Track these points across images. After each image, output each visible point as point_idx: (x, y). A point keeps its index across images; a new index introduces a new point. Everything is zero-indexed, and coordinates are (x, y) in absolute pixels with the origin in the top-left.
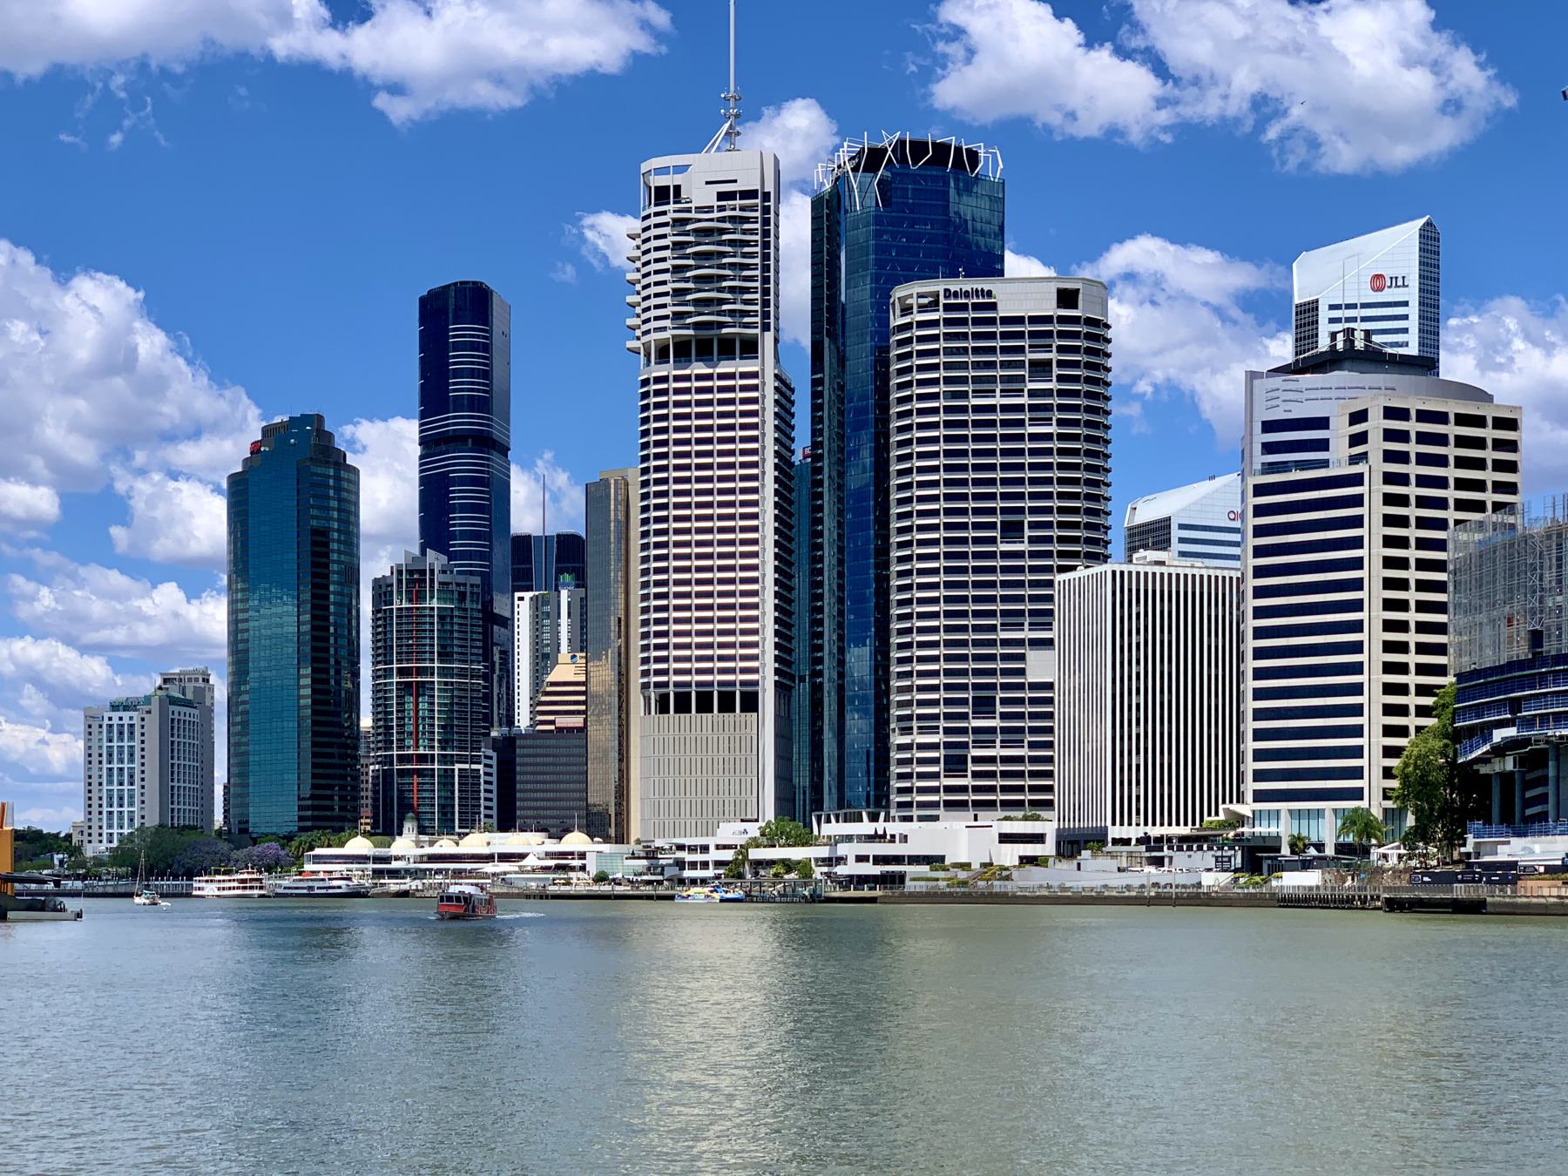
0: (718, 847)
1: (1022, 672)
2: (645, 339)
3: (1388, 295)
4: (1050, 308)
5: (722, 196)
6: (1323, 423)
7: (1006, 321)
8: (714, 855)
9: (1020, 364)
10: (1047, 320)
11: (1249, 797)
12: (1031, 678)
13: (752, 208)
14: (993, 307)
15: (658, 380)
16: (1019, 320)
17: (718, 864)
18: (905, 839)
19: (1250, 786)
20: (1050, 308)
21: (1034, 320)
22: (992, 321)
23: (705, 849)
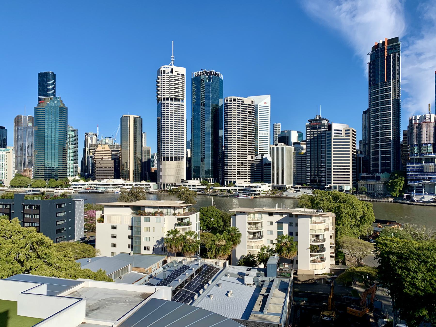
0: (197, 186)
1: (247, 159)
2: (163, 96)
3: (266, 105)
4: (251, 103)
5: (178, 74)
6: (341, 131)
7: (245, 104)
8: (196, 187)
9: (247, 111)
10: (250, 105)
11: (332, 183)
12: (248, 159)
13: (183, 77)
14: (243, 102)
15: (167, 104)
16: (247, 105)
17: (197, 188)
18: (260, 187)
19: (332, 182)
20: (251, 103)
21: (249, 105)
22: (243, 104)
23: (195, 186)
